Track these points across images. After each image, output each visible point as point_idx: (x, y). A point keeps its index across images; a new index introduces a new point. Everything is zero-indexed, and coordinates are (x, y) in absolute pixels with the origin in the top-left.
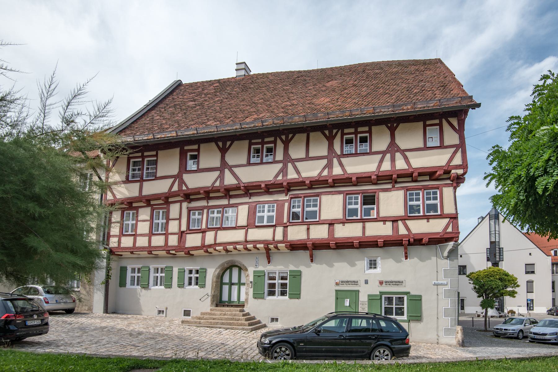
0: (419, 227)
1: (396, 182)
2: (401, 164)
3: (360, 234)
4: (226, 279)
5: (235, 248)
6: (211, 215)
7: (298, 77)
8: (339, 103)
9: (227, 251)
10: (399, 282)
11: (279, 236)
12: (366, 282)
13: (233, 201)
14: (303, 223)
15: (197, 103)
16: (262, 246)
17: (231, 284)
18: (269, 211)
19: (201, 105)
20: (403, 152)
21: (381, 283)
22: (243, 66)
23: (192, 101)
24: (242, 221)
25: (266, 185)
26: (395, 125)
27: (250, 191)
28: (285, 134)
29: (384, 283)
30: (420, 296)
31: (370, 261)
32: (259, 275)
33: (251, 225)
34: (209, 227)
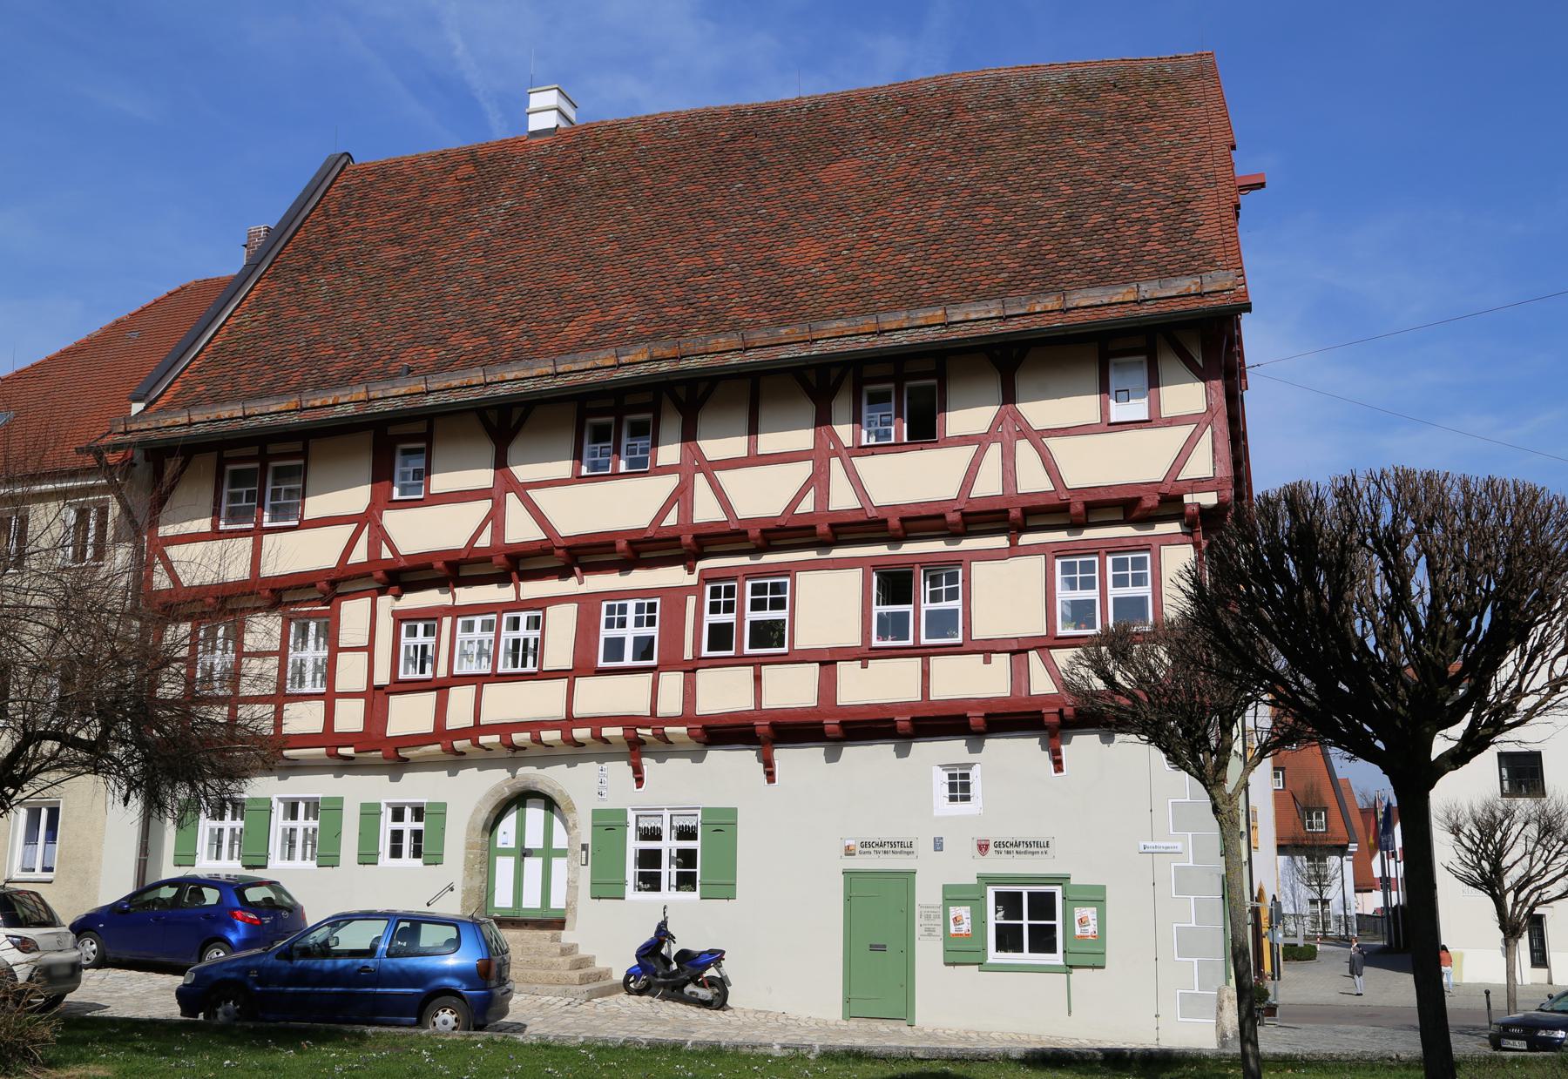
2: (1032, 480)
3: (914, 695)
5: (537, 740)
6: (461, 635)
10: (1037, 844)
11: (671, 703)
12: (938, 845)
13: (532, 589)
14: (740, 661)
18: (639, 623)
21: (983, 847)
23: (391, 242)
24: (559, 653)
29: (992, 848)
31: (951, 776)
32: (608, 824)
33: (583, 667)
34: (456, 671)
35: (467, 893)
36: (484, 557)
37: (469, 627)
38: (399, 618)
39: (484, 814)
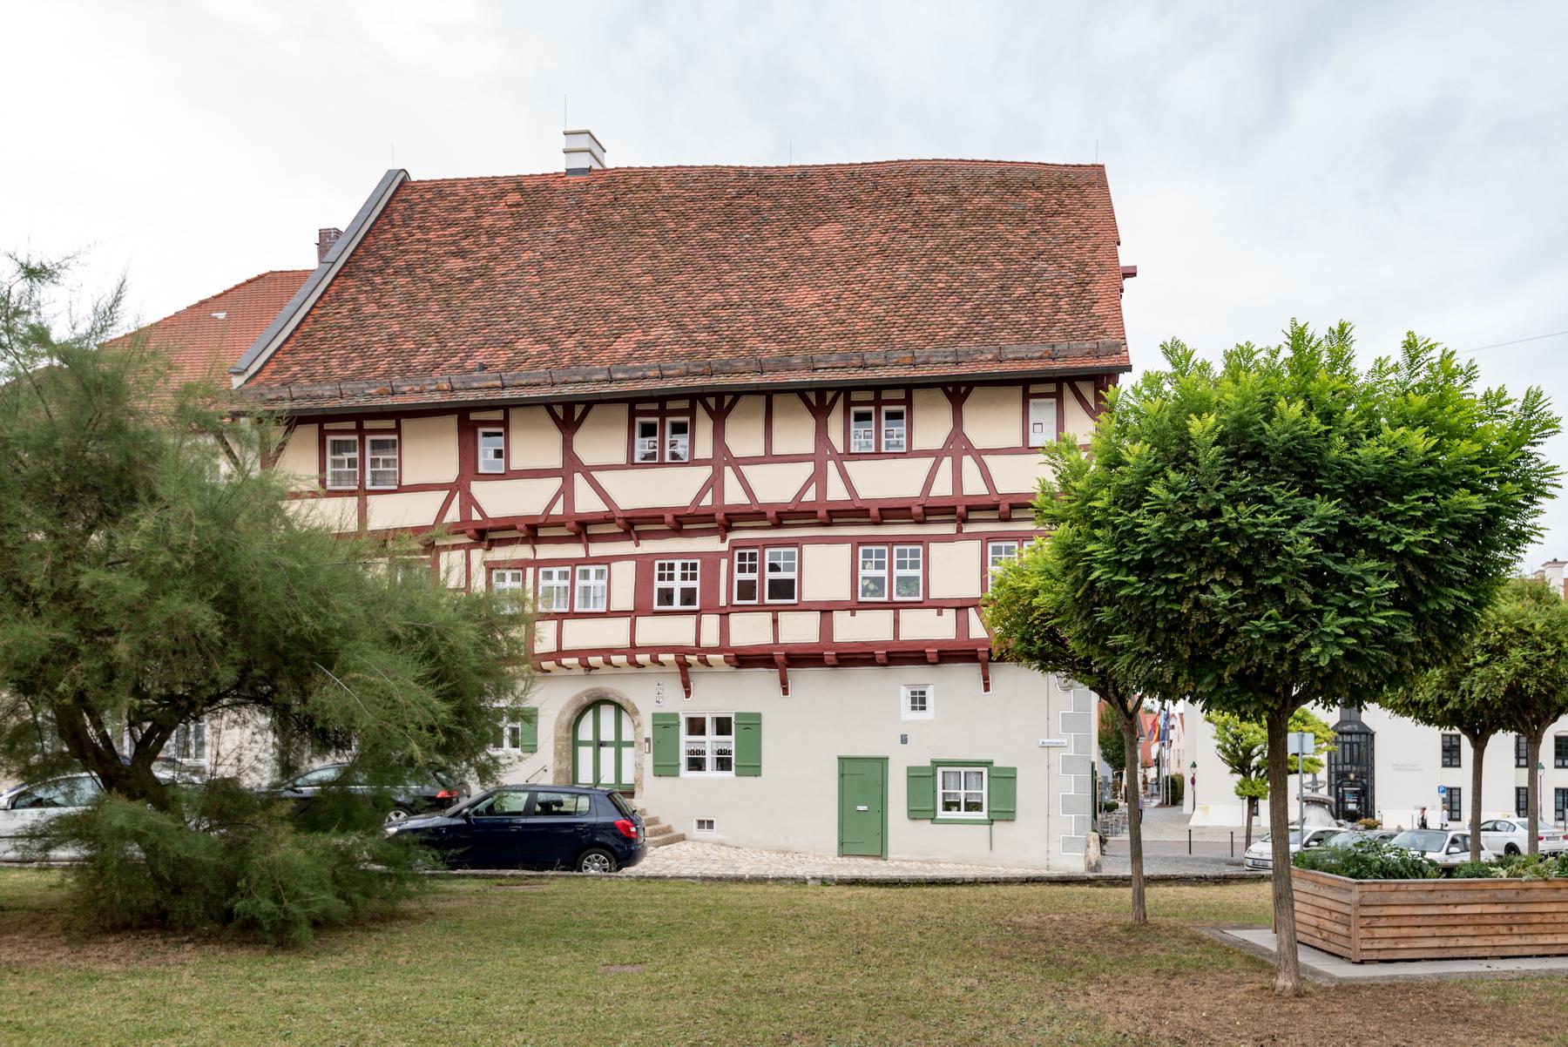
1: (965, 520)
2: (974, 486)
4: (586, 731)
5: (608, 663)
6: (543, 583)
8: (841, 314)
9: (589, 668)
11: (710, 637)
12: (904, 740)
13: (597, 550)
14: (762, 608)
15: (470, 264)
16: (670, 657)
18: (684, 577)
19: (485, 272)
20: (978, 454)
22: (584, 143)
23: (454, 255)
24: (624, 598)
25: (675, 517)
27: (638, 528)
28: (720, 404)
30: (1014, 770)
32: (665, 724)
33: (641, 609)
35: (558, 773)
36: (558, 523)
37: (549, 575)
38: (490, 567)
39: (569, 715)
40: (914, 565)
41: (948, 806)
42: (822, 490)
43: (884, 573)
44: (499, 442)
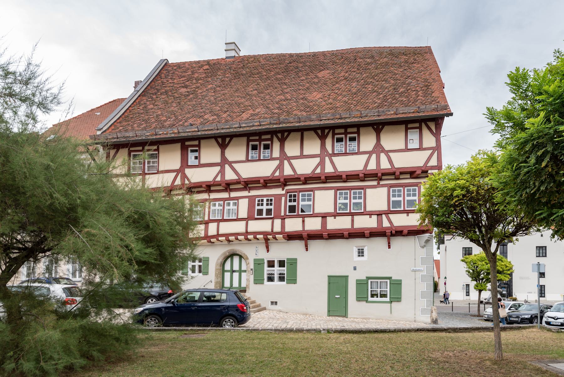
0: (400, 221)
1: (381, 179)
2: (385, 165)
3: (349, 226)
4: (228, 266)
5: (237, 239)
6: (212, 208)
7: (290, 63)
8: (331, 101)
9: (229, 241)
12: (355, 268)
13: (233, 194)
14: (298, 216)
15: (189, 90)
16: (262, 236)
17: (233, 271)
18: (267, 205)
19: (194, 92)
20: (387, 152)
22: (233, 47)
23: (183, 87)
24: (243, 213)
25: (264, 180)
26: (381, 127)
27: (250, 186)
28: (282, 135)
31: (359, 250)
32: (259, 263)
33: (250, 217)
34: (211, 218)
35: (216, 283)
37: (215, 205)
39: (221, 260)
40: (360, 198)
41: (372, 296)
42: (323, 168)
43: (348, 201)
44: (196, 154)
